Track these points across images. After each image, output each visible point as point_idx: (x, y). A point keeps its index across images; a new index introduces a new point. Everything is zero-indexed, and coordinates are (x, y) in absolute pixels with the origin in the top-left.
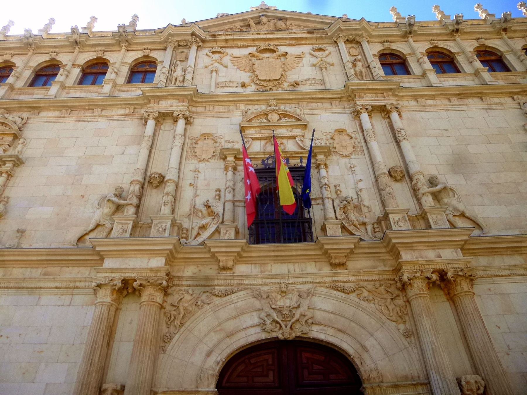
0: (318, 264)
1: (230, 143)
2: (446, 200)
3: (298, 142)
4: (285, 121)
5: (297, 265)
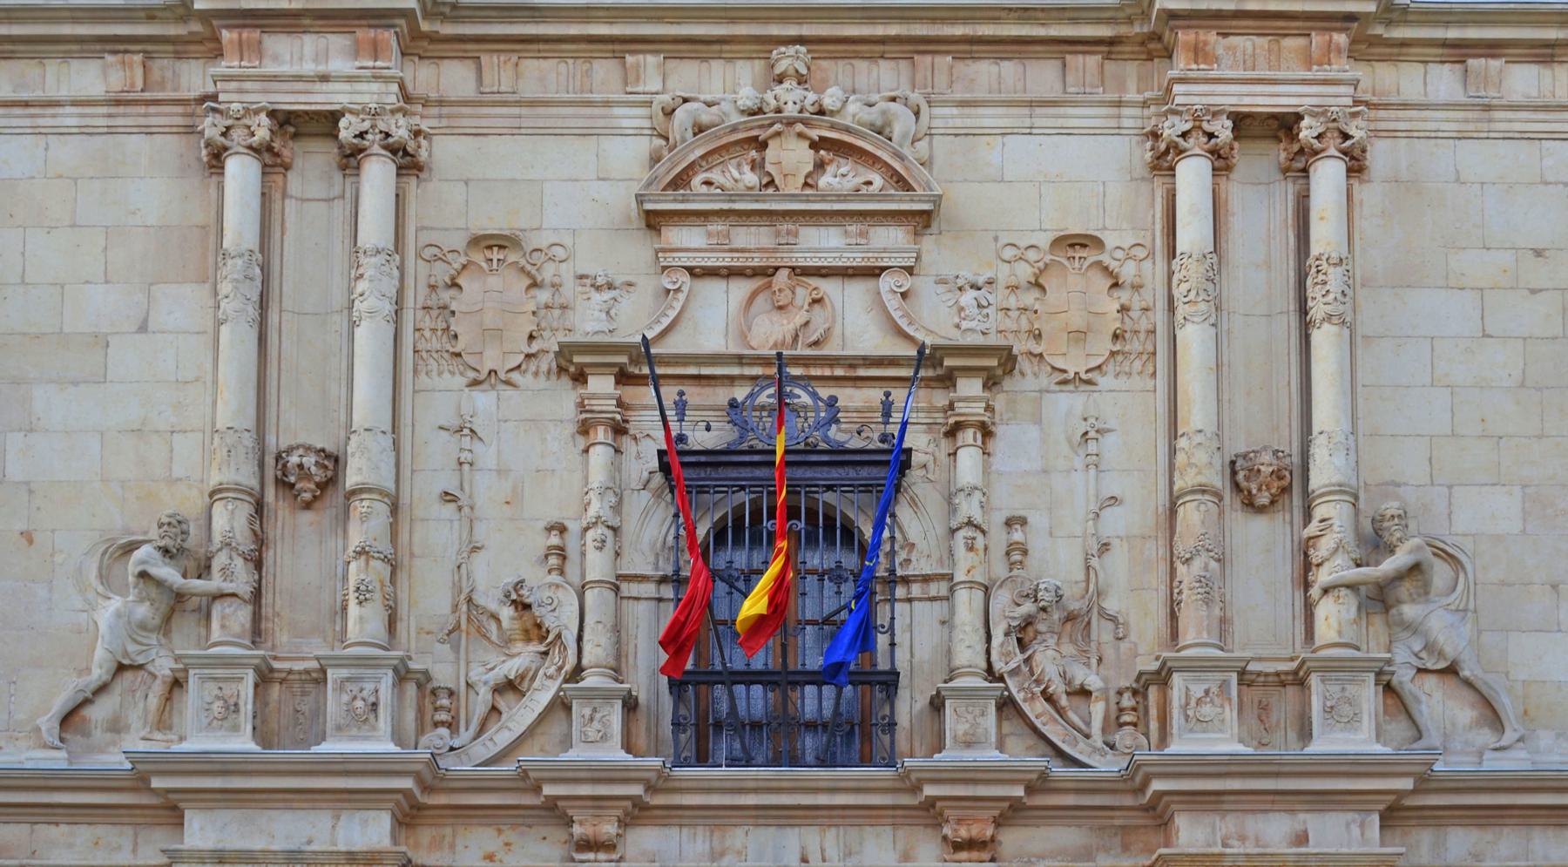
0: (901, 833)
1: (598, 288)
2: (1409, 611)
3: (886, 297)
4: (840, 177)
5: (831, 834)
